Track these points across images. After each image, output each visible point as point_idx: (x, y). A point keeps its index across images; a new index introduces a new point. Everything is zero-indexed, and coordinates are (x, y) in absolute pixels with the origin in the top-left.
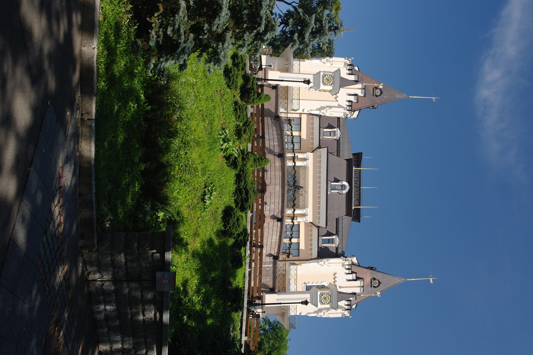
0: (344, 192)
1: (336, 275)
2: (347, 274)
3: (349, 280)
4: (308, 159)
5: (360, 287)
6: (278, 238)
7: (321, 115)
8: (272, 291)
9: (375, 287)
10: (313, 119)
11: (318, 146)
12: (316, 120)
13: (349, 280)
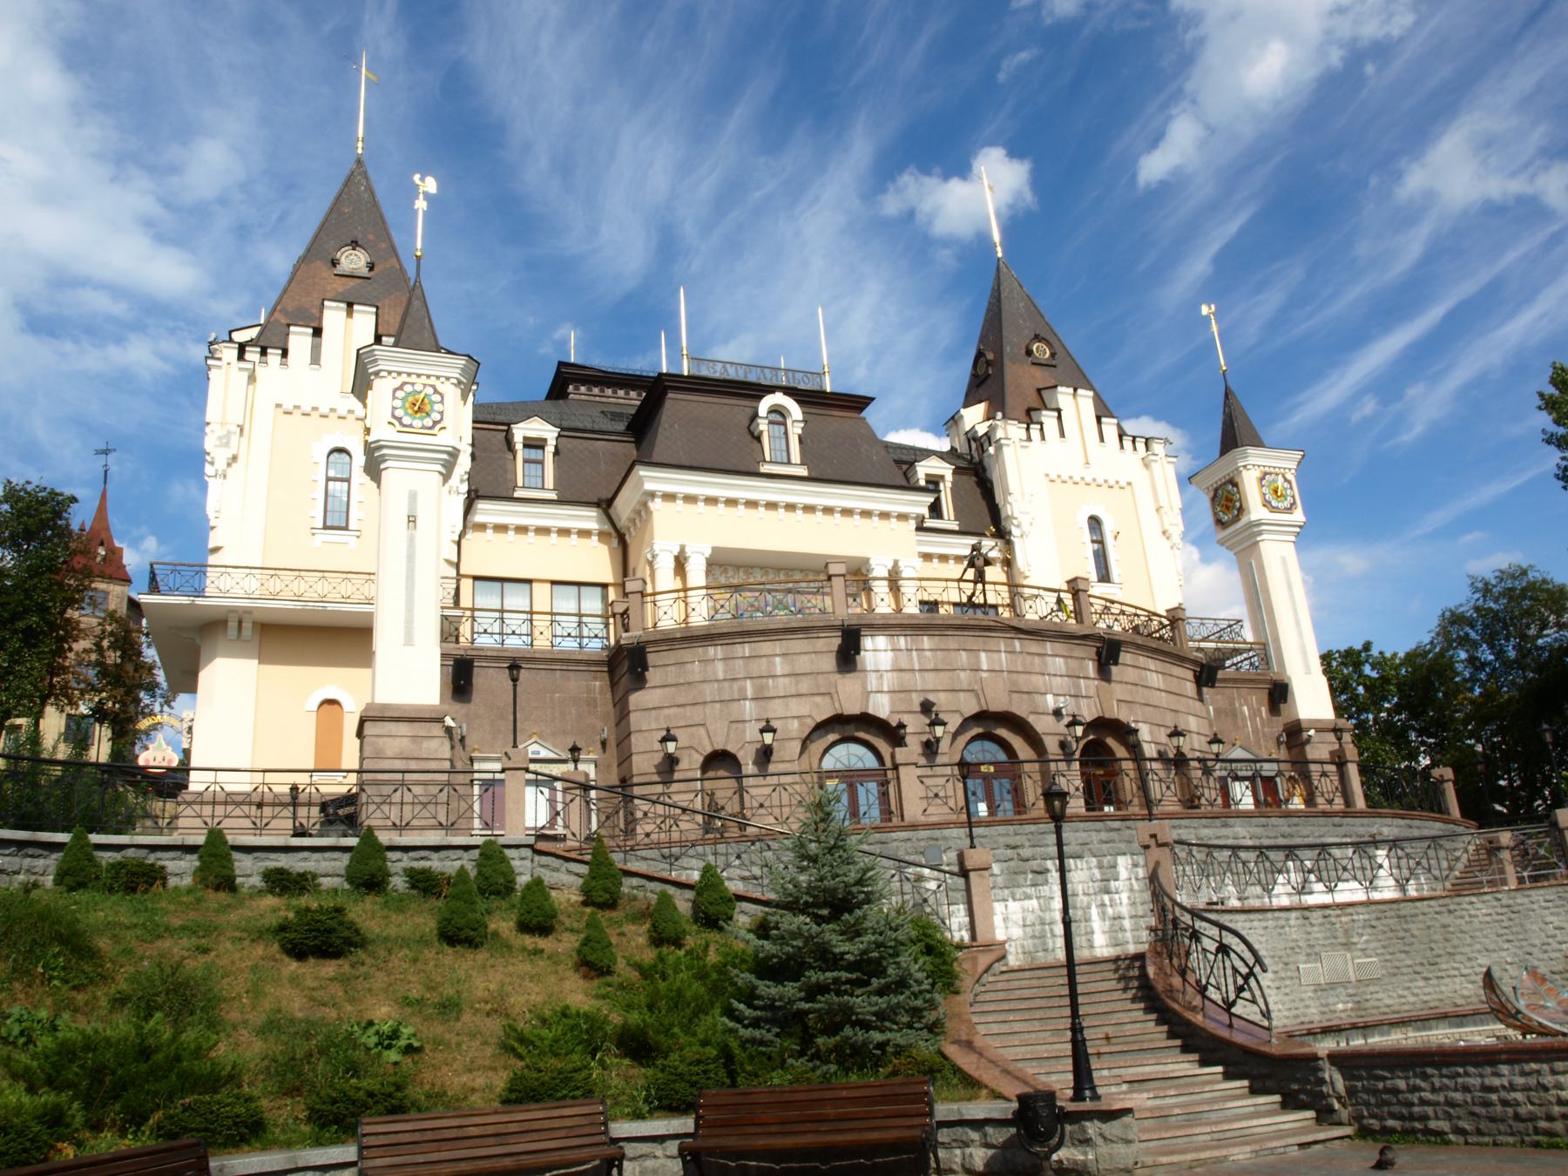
0: (795, 410)
1: (1053, 476)
2: (1043, 438)
3: (1062, 435)
4: (682, 549)
5: (1075, 395)
6: (1151, 664)
7: (469, 492)
8: (1279, 693)
9: (1053, 355)
10: (482, 527)
11: (593, 513)
12: (487, 511)
13: (1062, 435)
